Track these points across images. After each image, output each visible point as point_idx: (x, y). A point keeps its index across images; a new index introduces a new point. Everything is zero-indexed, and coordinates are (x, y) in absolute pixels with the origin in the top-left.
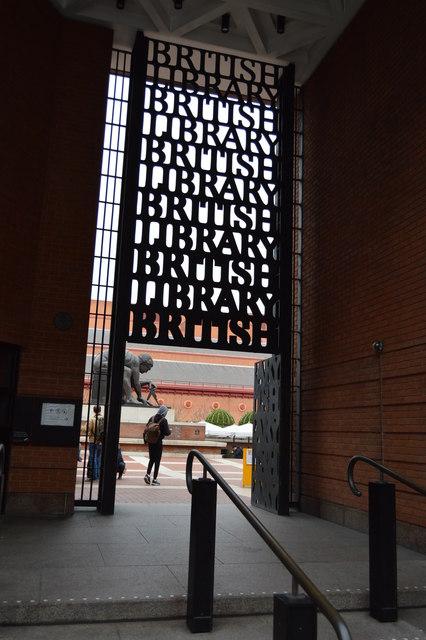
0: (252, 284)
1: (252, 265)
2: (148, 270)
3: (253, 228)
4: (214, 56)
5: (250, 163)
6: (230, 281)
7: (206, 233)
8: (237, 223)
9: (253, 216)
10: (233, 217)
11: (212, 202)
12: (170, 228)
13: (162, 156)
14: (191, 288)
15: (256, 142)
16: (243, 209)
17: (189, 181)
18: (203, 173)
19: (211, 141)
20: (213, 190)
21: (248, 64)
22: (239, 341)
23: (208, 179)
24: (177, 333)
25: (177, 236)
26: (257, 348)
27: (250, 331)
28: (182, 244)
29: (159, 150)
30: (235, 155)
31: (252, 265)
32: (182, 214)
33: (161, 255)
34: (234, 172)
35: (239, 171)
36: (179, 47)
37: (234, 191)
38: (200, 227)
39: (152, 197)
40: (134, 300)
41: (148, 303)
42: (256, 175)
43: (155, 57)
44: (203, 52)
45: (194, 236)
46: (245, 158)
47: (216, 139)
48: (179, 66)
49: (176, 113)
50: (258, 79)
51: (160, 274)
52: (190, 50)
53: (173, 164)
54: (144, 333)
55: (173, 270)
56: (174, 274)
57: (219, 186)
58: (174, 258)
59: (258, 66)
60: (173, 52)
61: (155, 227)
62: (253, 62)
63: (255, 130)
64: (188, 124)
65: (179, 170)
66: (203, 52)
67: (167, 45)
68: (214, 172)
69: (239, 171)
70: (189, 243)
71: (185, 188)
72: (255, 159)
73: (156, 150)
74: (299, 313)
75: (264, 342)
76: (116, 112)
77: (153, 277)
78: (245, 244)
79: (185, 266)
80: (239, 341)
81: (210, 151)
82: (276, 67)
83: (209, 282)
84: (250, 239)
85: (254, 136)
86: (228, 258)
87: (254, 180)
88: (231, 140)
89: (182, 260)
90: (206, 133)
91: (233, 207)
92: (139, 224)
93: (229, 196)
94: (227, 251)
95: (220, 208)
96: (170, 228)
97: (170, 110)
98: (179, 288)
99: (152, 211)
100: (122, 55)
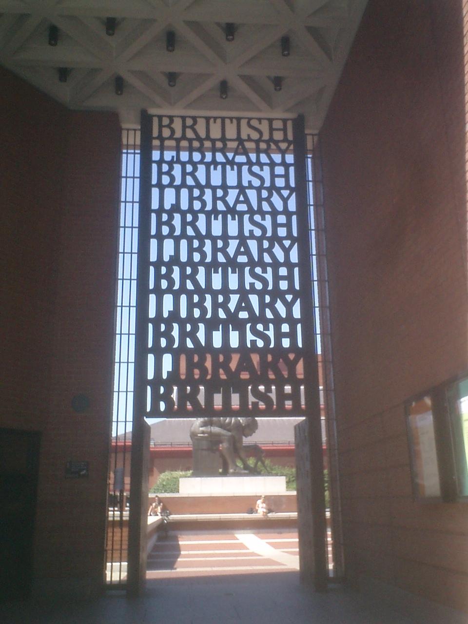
0: (272, 346)
1: (271, 326)
2: (163, 342)
3: (270, 287)
4: (219, 121)
5: (263, 222)
6: (249, 345)
7: (221, 299)
8: (252, 285)
9: (269, 276)
10: (248, 279)
11: (225, 267)
12: (183, 299)
13: (172, 229)
15: (268, 199)
16: (258, 270)
17: (200, 250)
18: (214, 240)
19: (221, 206)
20: (226, 255)
21: (254, 123)
22: (262, 405)
23: (220, 244)
24: (195, 403)
25: (191, 306)
26: (281, 412)
27: (273, 396)
28: (197, 313)
29: (169, 223)
30: (246, 217)
31: (271, 326)
32: (195, 283)
33: (176, 326)
34: (247, 234)
35: (251, 232)
36: (184, 118)
37: (248, 253)
38: (214, 294)
39: (164, 270)
40: (151, 375)
41: (165, 376)
42: (269, 234)
43: (160, 132)
44: (208, 119)
45: (208, 304)
46: (257, 218)
47: (226, 204)
49: (184, 184)
50: (266, 136)
51: (176, 345)
52: (194, 119)
53: (184, 235)
54: (162, 406)
57: (231, 250)
58: (189, 327)
59: (265, 124)
60: (177, 125)
61: (168, 300)
62: (260, 120)
63: (266, 188)
64: (196, 193)
65: (190, 240)
66: (208, 119)
67: (171, 118)
68: (225, 237)
69: (251, 232)
70: (204, 311)
72: (268, 217)
73: (166, 223)
74: (332, 369)
75: (288, 404)
76: (130, 190)
77: (169, 349)
78: (263, 305)
79: (201, 335)
80: (262, 405)
81: (220, 216)
82: (285, 121)
84: (268, 299)
85: (265, 194)
86: (245, 321)
87: (268, 239)
88: (242, 202)
90: (215, 199)
91: (247, 269)
92: (152, 298)
93: (243, 259)
94: (244, 315)
95: (233, 272)
96: (183, 299)
97: (178, 182)
99: (164, 284)
100: (131, 133)
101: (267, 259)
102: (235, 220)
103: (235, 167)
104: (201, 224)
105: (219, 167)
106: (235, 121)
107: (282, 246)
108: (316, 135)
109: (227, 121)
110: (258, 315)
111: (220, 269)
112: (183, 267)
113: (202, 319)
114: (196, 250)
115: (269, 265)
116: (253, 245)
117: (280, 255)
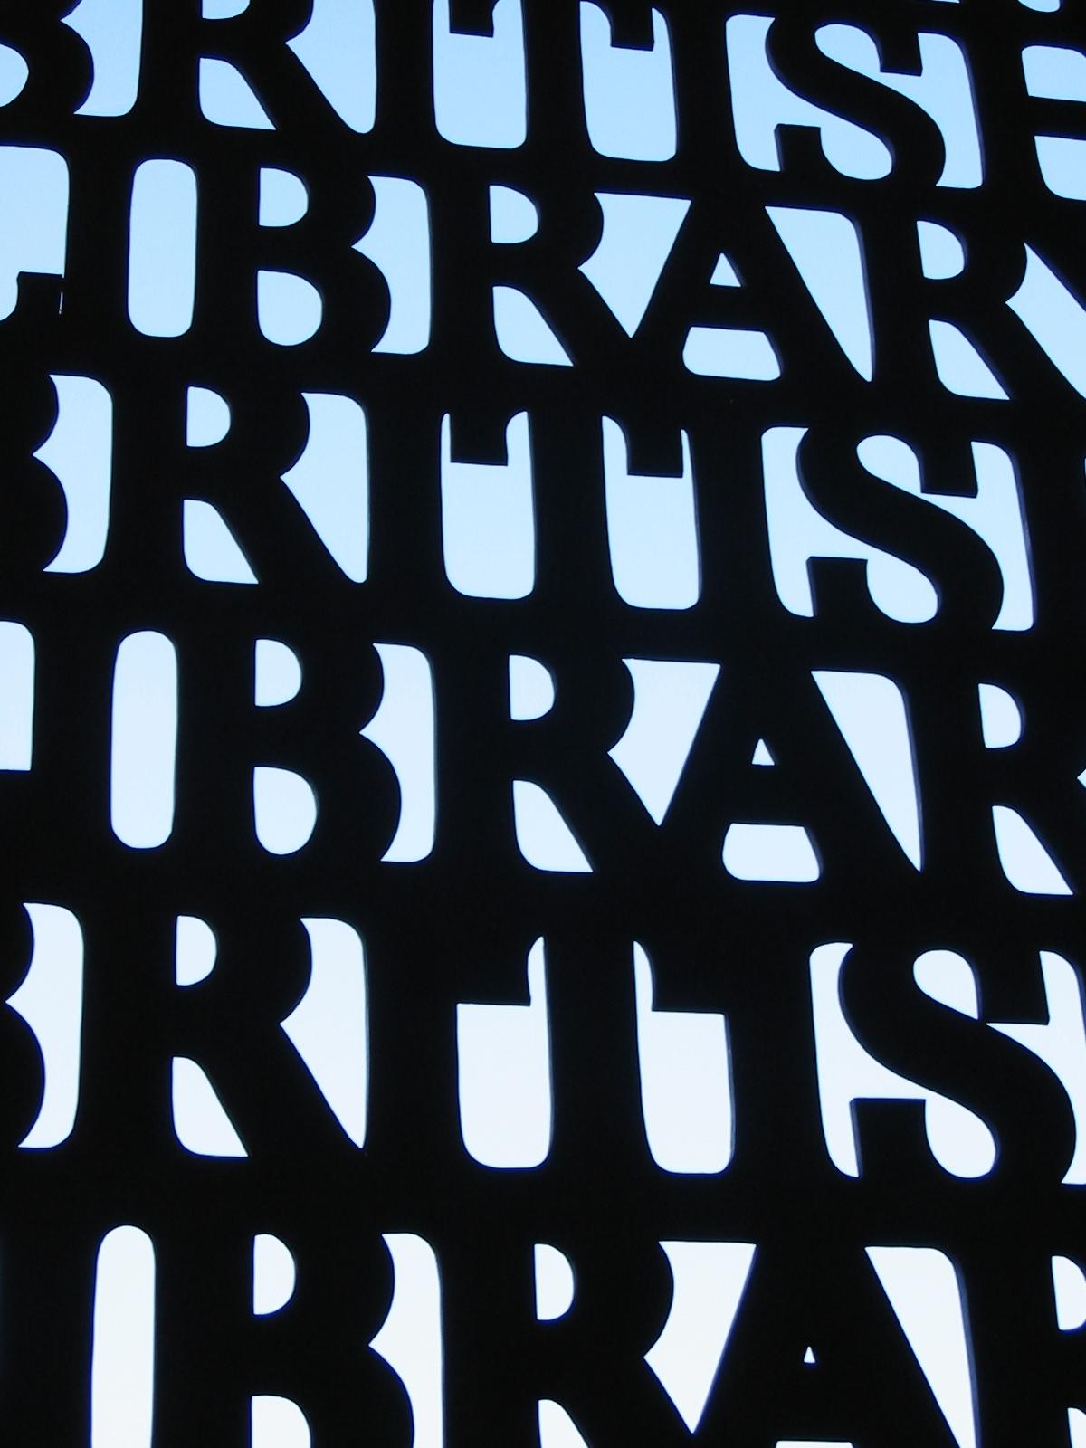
6: (844, 1153)
7: (531, 690)
10: (798, 535)
12: (146, 672)
14: (414, 1262)
16: (890, 460)
18: (457, 181)
23: (513, 217)
25: (220, 743)
28: (284, 810)
32: (274, 528)
34: (759, 151)
35: (798, 144)
42: (963, 167)
55: (190, 1085)
56: (202, 1120)
58: (195, 950)
65: (226, 167)
70: (356, 793)
71: (289, 309)
79: (331, 1031)
83: (603, 1184)
86: (788, 917)
87: (955, 210)
89: (290, 974)
91: (781, 448)
93: (730, 354)
94: (770, 853)
95: (651, 459)
96: (146, 672)
98: (274, 1275)
101: (961, 367)
110: (912, 849)
111: (518, 430)
113: (343, 863)
114: (287, 249)
115: (979, 419)
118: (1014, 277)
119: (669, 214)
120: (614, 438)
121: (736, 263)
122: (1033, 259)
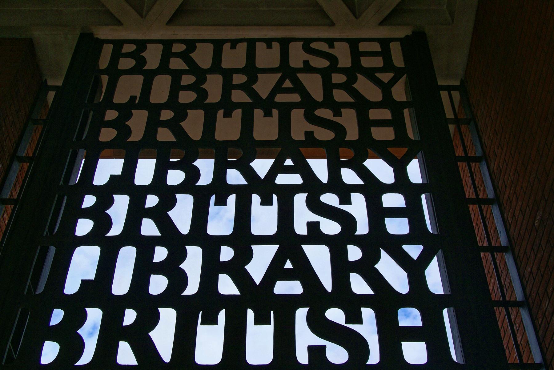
11: (235, 309)
16: (336, 315)
18: (210, 246)
20: (241, 277)
30: (300, 199)
34: (301, 229)
35: (313, 227)
37: (304, 272)
42: (363, 228)
48: (164, 68)
52: (191, 45)
57: (257, 269)
65: (145, 246)
81: (232, 199)
82: (385, 43)
87: (359, 241)
91: (301, 314)
95: (261, 320)
101: (359, 285)
102: (271, 204)
103: (275, 112)
104: (182, 215)
105: (238, 114)
106: (276, 46)
107: (402, 259)
108: (454, 88)
109: (260, 47)
112: (113, 307)
115: (364, 300)
116: (319, 257)
117: (396, 277)
118: (377, 258)
119: (273, 249)
120: (250, 314)
121: (292, 262)
122: (382, 251)
